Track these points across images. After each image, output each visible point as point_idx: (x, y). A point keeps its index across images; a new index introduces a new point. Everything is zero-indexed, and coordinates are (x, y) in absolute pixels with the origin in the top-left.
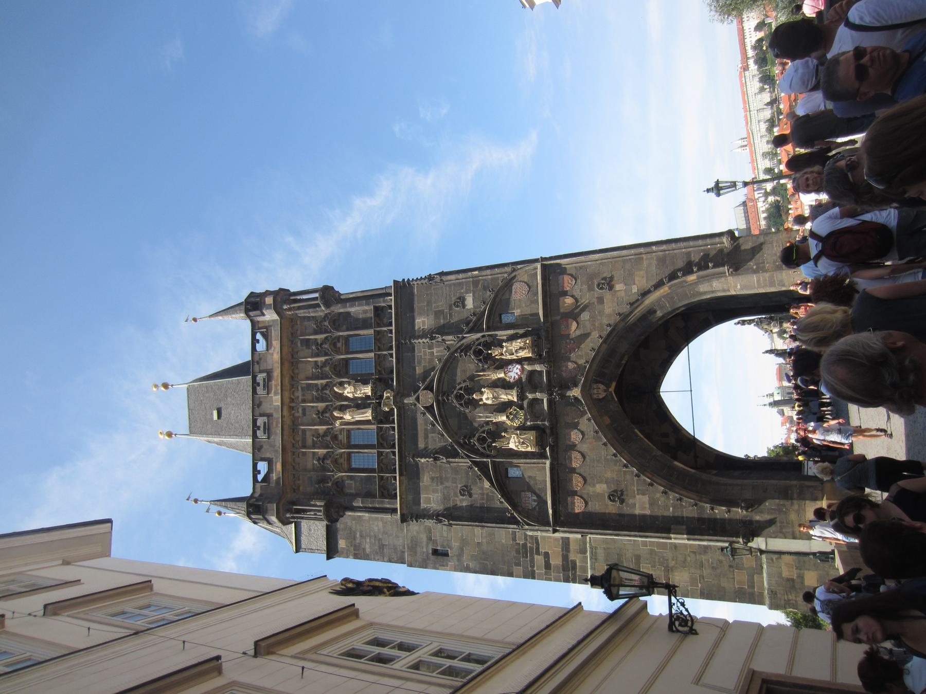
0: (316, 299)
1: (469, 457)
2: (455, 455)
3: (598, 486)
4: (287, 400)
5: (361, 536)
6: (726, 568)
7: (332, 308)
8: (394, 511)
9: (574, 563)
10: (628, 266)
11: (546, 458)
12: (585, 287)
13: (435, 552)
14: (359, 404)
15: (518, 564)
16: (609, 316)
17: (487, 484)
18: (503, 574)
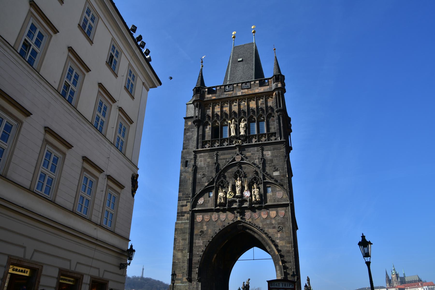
0: (280, 106)
1: (216, 177)
2: (217, 171)
3: (206, 227)
4: (239, 98)
5: (192, 131)
6: (183, 271)
7: (276, 113)
8: (197, 148)
9: (184, 216)
10: (287, 238)
11: (215, 207)
12: (280, 221)
13: (187, 162)
14: (237, 130)
15: (183, 195)
16: (268, 231)
17: (206, 184)
18: (179, 189)
